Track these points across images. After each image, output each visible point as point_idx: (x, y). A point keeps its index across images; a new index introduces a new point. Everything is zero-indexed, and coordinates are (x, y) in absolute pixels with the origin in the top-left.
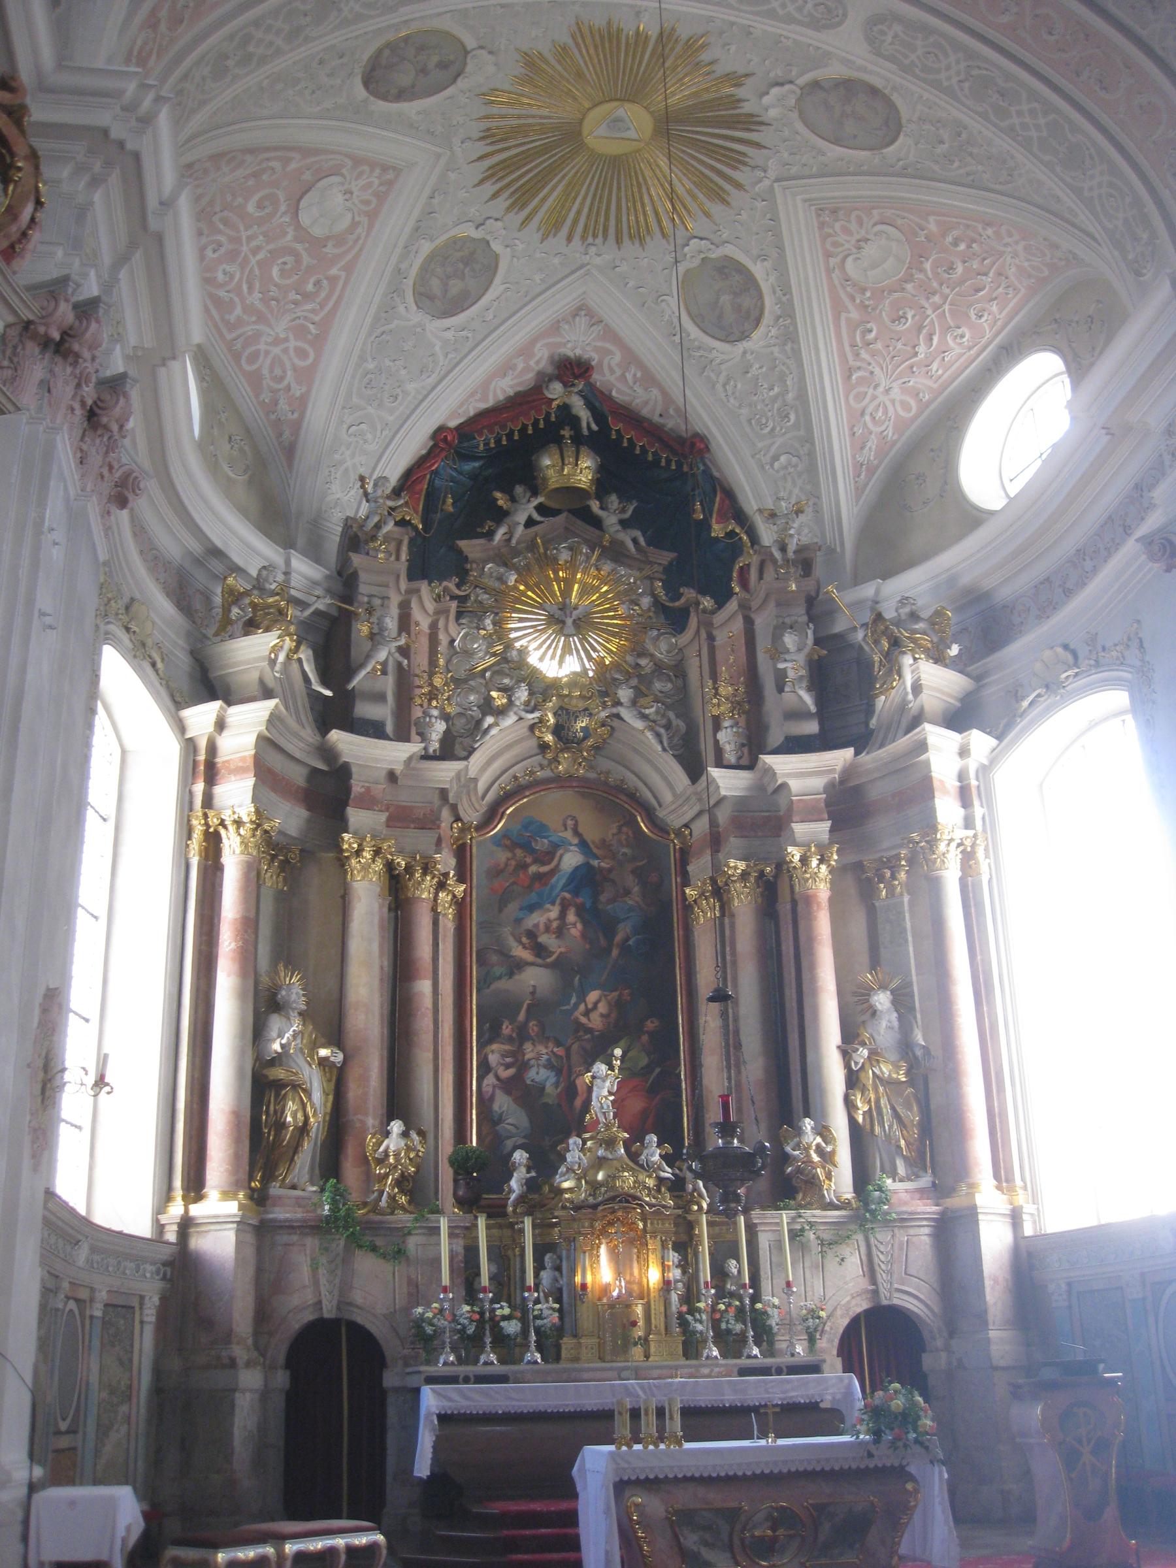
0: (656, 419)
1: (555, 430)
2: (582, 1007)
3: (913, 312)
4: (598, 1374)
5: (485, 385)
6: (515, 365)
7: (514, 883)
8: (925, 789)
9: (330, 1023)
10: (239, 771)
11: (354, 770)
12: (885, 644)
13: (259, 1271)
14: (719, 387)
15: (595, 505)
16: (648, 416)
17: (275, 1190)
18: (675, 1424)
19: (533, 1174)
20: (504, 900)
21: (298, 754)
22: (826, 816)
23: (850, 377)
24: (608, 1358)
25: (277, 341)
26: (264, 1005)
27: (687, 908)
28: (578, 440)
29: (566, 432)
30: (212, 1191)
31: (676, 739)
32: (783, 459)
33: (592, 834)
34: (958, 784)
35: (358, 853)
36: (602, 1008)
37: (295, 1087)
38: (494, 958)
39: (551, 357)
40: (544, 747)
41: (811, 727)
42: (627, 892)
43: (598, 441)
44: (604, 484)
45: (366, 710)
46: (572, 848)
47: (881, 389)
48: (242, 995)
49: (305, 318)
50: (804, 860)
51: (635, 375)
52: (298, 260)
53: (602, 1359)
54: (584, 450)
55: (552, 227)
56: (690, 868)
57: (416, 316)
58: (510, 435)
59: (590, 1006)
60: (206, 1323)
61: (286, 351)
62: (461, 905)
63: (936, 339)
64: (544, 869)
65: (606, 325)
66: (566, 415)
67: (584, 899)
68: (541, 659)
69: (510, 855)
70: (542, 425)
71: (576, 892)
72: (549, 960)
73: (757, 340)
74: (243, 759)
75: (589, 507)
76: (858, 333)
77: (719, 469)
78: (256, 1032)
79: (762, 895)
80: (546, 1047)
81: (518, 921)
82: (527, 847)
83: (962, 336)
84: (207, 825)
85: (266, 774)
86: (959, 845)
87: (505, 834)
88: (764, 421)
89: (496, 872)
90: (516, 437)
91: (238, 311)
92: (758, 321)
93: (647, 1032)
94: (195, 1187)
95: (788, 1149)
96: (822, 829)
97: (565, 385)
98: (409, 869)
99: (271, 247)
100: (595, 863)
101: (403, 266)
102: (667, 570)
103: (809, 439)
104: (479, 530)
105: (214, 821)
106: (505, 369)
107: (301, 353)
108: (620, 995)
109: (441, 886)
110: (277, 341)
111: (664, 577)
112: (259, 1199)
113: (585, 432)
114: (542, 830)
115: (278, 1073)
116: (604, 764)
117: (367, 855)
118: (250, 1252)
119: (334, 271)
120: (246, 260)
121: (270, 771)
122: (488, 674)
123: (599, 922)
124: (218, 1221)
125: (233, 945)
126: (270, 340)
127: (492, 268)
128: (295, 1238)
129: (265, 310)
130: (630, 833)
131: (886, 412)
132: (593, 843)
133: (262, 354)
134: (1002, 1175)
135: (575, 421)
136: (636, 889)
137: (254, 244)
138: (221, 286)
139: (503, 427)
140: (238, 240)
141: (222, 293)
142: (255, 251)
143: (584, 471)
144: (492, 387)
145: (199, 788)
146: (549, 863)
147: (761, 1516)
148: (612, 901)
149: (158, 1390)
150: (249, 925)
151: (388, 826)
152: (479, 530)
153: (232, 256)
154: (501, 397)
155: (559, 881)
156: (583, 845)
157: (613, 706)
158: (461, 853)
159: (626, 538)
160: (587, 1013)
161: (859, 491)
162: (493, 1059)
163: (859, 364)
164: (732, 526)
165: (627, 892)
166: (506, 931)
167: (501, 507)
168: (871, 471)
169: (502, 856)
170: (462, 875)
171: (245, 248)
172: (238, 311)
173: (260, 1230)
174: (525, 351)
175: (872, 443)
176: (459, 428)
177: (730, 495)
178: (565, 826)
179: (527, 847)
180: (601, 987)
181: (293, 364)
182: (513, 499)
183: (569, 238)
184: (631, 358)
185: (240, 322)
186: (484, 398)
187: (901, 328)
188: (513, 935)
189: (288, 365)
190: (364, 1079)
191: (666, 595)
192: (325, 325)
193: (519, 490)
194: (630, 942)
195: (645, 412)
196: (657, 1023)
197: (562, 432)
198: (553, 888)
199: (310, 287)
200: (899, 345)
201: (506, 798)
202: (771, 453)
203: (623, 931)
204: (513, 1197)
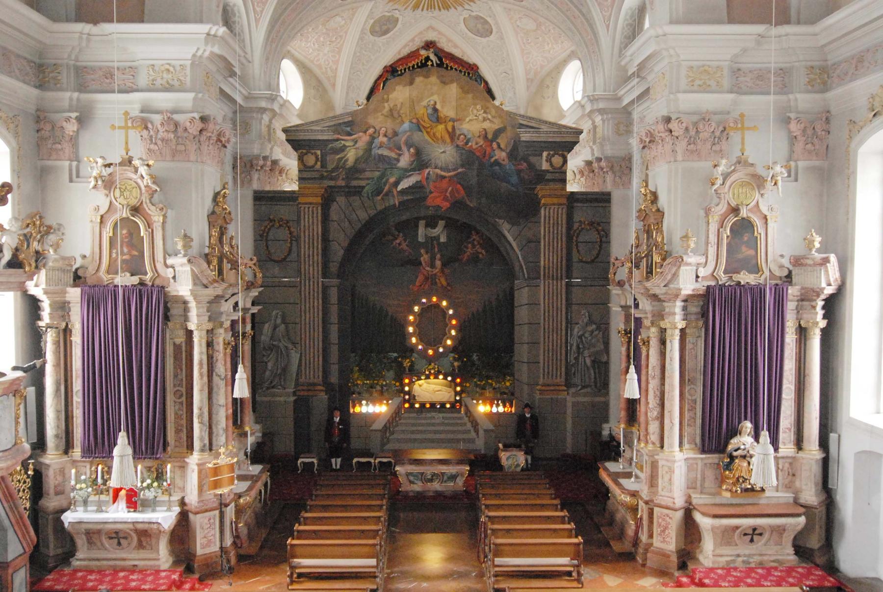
5: (399, 53)
66: (428, 59)
92: (491, 33)
127: (397, 20)
174: (413, 40)
176: (391, 66)
183: (422, 10)
184: (449, 41)
195: (456, 55)
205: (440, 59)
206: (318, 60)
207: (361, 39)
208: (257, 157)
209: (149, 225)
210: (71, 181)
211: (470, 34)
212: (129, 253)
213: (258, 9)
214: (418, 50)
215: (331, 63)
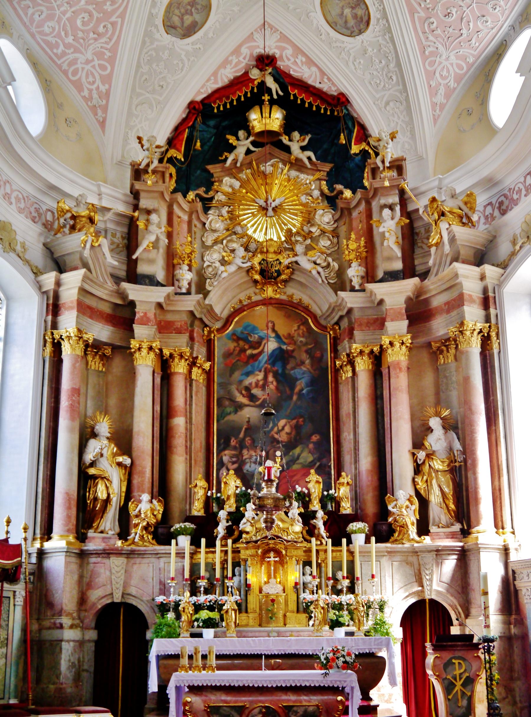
0: (317, 85)
1: (257, 97)
2: (276, 429)
3: (455, 9)
4: (257, 634)
5: (215, 74)
6: (232, 60)
7: (238, 360)
8: (458, 302)
10: (71, 308)
11: (137, 303)
12: (436, 216)
13: (81, 577)
14: (350, 64)
15: (285, 139)
16: (313, 84)
17: (91, 533)
18: (213, 661)
19: (230, 523)
20: (231, 369)
21: (104, 297)
22: (405, 317)
23: (424, 52)
24: (263, 625)
25: (88, 62)
26: (86, 435)
27: (337, 371)
28: (272, 102)
29: (266, 98)
31: (332, 274)
32: (391, 104)
33: (282, 331)
34: (482, 296)
35: (139, 349)
36: (287, 429)
37: (103, 478)
38: (227, 403)
39: (251, 55)
40: (256, 282)
41: (398, 265)
42: (303, 363)
43: (282, 102)
44: (288, 127)
46: (271, 339)
47: (444, 57)
48: (71, 430)
49: (102, 47)
50: (391, 344)
51: (301, 61)
52: (91, 15)
53: (260, 625)
54: (275, 108)
56: (339, 348)
57: (167, 39)
58: (231, 103)
59: (280, 428)
60: (50, 605)
61: (93, 67)
62: (209, 375)
63: (471, 25)
64: (255, 352)
65: (281, 32)
66: (263, 87)
67: (278, 367)
68: (255, 231)
69: (236, 344)
70: (249, 95)
71: (273, 364)
72: (258, 403)
73: (368, 35)
74: (72, 302)
75: (281, 141)
76: (426, 25)
77: (356, 112)
79: (372, 363)
80: (255, 452)
81: (241, 382)
82: (246, 340)
83: (487, 22)
84: (54, 339)
86: (479, 333)
87: (234, 334)
88: (378, 82)
89: (228, 355)
90: (235, 103)
91: (62, 47)
92: (368, 23)
93: (313, 443)
94: (47, 533)
95: (390, 508)
97: (261, 70)
98: (171, 355)
99: (73, 9)
100: (284, 347)
101: (154, 11)
102: (329, 174)
104: (220, 158)
105: (57, 337)
106: (225, 63)
107: (103, 67)
108: (297, 422)
109: (193, 364)
110: (88, 62)
111: (327, 178)
112: (82, 538)
113: (275, 97)
114: (254, 329)
115: (92, 471)
117: (144, 351)
118: (74, 567)
119: (113, 19)
120: (60, 19)
121: (90, 308)
122: (225, 242)
123: (285, 381)
125: (67, 404)
126: (83, 61)
128: (99, 559)
129: (77, 45)
130: (305, 330)
131: (448, 71)
132: (284, 336)
133: (80, 70)
134: (499, 524)
135: (269, 91)
136: (308, 362)
137: (62, 9)
138: (47, 35)
139: (228, 98)
140: (53, 9)
141: (49, 38)
142: (64, 13)
143: (275, 120)
144: (219, 76)
145: (50, 318)
146: (258, 348)
147: (256, 711)
148: (293, 368)
149: (24, 640)
150: (75, 391)
151: (160, 333)
152: (220, 158)
153: (51, 17)
154: (226, 81)
155: (264, 358)
156: (278, 337)
157: (293, 257)
158: (209, 344)
159: (304, 156)
160: (279, 431)
161: (435, 121)
162: (225, 459)
163: (429, 43)
164: (364, 146)
165: (303, 363)
166: (233, 388)
167: (232, 144)
168: (442, 107)
169: (232, 345)
170: (210, 357)
171: (58, 12)
172: (62, 47)
174: (236, 51)
175: (442, 91)
177: (363, 128)
178: (267, 326)
179: (246, 340)
180: (287, 417)
181: (100, 74)
182: (238, 139)
185: (64, 54)
186: (216, 82)
187: (450, 20)
188: (237, 389)
189: (96, 75)
190: (143, 473)
191: (329, 189)
192: (114, 50)
194: (304, 392)
195: (310, 82)
196: (318, 437)
197: (263, 98)
198: (260, 362)
199: (101, 29)
200: (451, 30)
201: (236, 312)
202: (385, 99)
203: (301, 385)
204: (220, 536)
206: (75, 73)
207: (148, 34)
211: (333, 33)
214: (246, 74)
215: (98, 82)
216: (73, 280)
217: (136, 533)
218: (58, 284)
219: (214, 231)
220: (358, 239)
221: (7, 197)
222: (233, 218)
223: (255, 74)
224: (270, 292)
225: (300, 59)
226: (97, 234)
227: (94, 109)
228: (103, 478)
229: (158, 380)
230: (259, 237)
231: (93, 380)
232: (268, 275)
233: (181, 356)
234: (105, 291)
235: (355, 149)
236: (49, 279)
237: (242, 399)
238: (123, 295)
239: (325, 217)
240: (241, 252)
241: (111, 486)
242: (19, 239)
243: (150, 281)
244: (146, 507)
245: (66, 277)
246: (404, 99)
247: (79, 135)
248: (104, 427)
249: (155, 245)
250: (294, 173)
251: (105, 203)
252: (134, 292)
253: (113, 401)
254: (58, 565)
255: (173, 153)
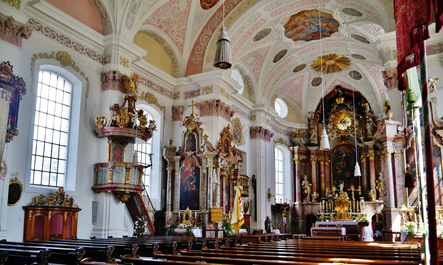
9: (310, 180)
13: (302, 209)
17: (304, 200)
26: (302, 180)
28: (342, 96)
30: (297, 201)
37: (306, 189)
43: (343, 96)
44: (345, 101)
45: (312, 142)
48: (298, 179)
55: (328, 72)
57: (313, 87)
62: (330, 163)
66: (338, 93)
78: (301, 183)
85: (299, 153)
89: (334, 158)
94: (295, 201)
96: (373, 151)
103: (373, 90)
114: (340, 152)
115: (304, 187)
116: (349, 141)
118: (301, 207)
124: (297, 204)
127: (321, 79)
143: (342, 100)
150: (299, 171)
153: (286, 91)
156: (346, 153)
158: (330, 156)
169: (335, 156)
173: (302, 205)
174: (331, 86)
177: (365, 99)
184: (346, 84)
190: (314, 187)
192: (301, 93)
193: (335, 104)
205: (343, 92)
208: (257, 127)
209: (198, 135)
210: (180, 126)
212: (192, 145)
213: (257, 76)
214: (334, 90)
216: (296, 148)
217: (313, 200)
218: (293, 149)
219: (330, 128)
220: (362, 130)
221: (281, 133)
222: (334, 126)
223: (336, 90)
224: (343, 142)
225: (347, 85)
226: (300, 138)
227: (298, 105)
228: (306, 189)
229: (317, 166)
230: (340, 128)
231: (303, 167)
232: (343, 138)
233: (322, 160)
234: (303, 149)
235: (363, 105)
236: (291, 148)
237: (338, 168)
238: (308, 149)
239: (356, 123)
240: (336, 134)
241: (308, 191)
242: (284, 140)
243: (314, 145)
244: (315, 194)
245: (295, 147)
246: (373, 92)
247: (296, 112)
248: (306, 178)
249: (314, 136)
250: (348, 112)
251: (303, 128)
252: (310, 148)
253: (308, 172)
254: (297, 207)
255: (318, 111)
